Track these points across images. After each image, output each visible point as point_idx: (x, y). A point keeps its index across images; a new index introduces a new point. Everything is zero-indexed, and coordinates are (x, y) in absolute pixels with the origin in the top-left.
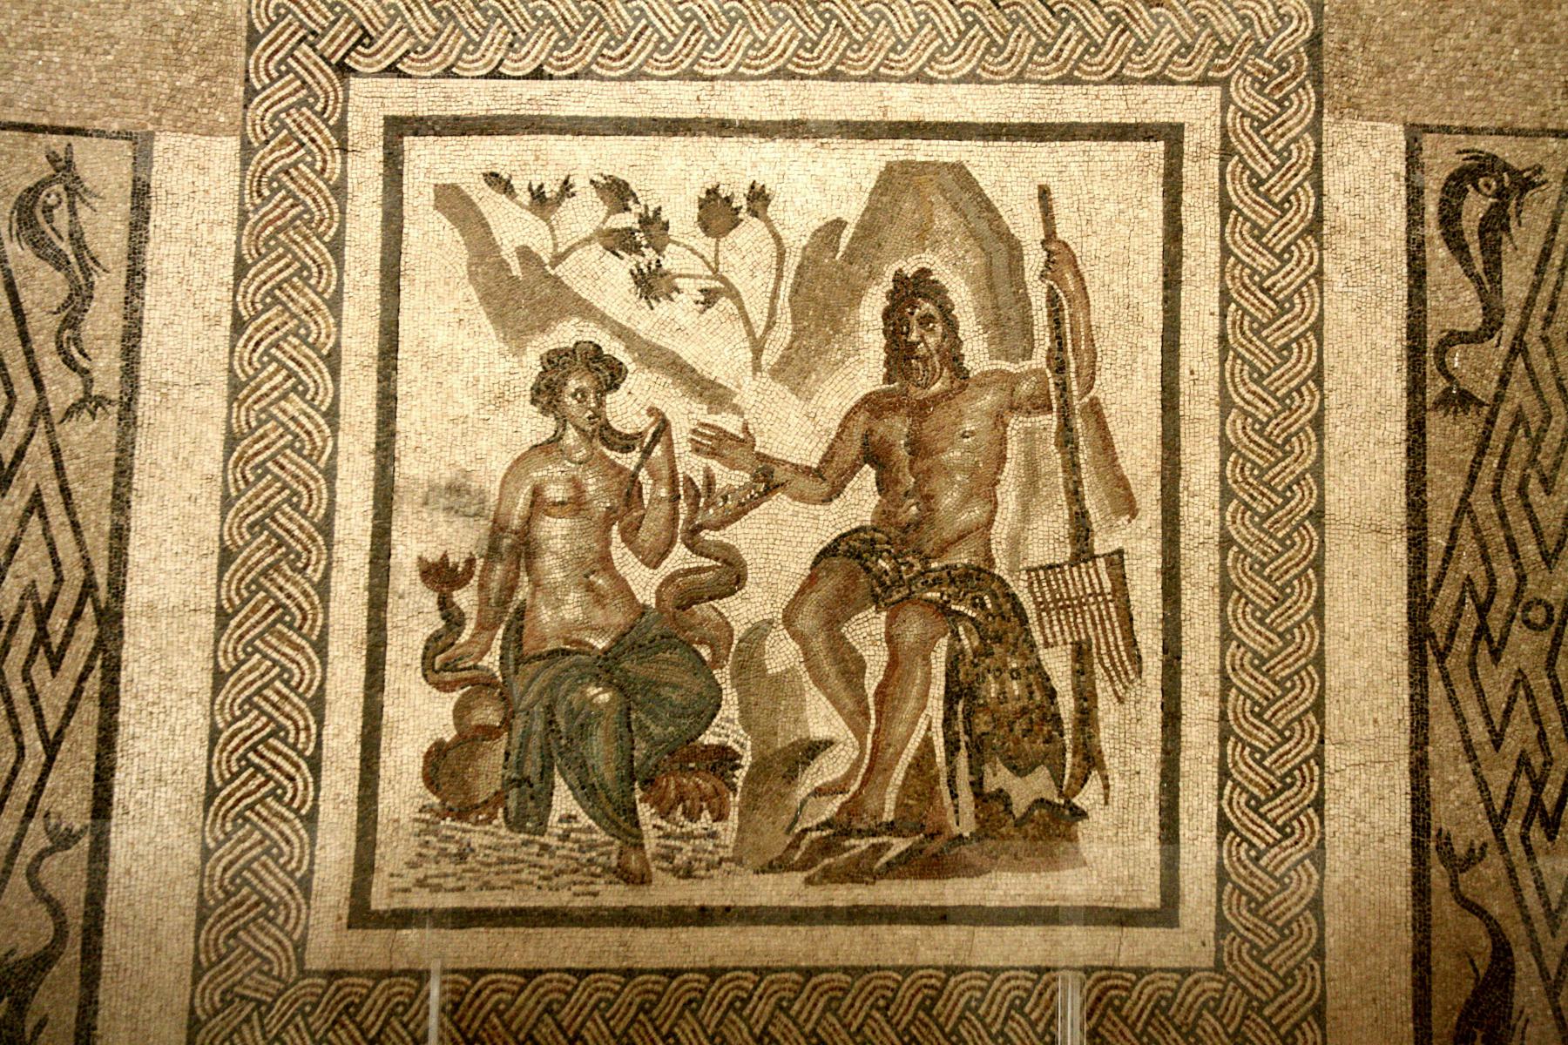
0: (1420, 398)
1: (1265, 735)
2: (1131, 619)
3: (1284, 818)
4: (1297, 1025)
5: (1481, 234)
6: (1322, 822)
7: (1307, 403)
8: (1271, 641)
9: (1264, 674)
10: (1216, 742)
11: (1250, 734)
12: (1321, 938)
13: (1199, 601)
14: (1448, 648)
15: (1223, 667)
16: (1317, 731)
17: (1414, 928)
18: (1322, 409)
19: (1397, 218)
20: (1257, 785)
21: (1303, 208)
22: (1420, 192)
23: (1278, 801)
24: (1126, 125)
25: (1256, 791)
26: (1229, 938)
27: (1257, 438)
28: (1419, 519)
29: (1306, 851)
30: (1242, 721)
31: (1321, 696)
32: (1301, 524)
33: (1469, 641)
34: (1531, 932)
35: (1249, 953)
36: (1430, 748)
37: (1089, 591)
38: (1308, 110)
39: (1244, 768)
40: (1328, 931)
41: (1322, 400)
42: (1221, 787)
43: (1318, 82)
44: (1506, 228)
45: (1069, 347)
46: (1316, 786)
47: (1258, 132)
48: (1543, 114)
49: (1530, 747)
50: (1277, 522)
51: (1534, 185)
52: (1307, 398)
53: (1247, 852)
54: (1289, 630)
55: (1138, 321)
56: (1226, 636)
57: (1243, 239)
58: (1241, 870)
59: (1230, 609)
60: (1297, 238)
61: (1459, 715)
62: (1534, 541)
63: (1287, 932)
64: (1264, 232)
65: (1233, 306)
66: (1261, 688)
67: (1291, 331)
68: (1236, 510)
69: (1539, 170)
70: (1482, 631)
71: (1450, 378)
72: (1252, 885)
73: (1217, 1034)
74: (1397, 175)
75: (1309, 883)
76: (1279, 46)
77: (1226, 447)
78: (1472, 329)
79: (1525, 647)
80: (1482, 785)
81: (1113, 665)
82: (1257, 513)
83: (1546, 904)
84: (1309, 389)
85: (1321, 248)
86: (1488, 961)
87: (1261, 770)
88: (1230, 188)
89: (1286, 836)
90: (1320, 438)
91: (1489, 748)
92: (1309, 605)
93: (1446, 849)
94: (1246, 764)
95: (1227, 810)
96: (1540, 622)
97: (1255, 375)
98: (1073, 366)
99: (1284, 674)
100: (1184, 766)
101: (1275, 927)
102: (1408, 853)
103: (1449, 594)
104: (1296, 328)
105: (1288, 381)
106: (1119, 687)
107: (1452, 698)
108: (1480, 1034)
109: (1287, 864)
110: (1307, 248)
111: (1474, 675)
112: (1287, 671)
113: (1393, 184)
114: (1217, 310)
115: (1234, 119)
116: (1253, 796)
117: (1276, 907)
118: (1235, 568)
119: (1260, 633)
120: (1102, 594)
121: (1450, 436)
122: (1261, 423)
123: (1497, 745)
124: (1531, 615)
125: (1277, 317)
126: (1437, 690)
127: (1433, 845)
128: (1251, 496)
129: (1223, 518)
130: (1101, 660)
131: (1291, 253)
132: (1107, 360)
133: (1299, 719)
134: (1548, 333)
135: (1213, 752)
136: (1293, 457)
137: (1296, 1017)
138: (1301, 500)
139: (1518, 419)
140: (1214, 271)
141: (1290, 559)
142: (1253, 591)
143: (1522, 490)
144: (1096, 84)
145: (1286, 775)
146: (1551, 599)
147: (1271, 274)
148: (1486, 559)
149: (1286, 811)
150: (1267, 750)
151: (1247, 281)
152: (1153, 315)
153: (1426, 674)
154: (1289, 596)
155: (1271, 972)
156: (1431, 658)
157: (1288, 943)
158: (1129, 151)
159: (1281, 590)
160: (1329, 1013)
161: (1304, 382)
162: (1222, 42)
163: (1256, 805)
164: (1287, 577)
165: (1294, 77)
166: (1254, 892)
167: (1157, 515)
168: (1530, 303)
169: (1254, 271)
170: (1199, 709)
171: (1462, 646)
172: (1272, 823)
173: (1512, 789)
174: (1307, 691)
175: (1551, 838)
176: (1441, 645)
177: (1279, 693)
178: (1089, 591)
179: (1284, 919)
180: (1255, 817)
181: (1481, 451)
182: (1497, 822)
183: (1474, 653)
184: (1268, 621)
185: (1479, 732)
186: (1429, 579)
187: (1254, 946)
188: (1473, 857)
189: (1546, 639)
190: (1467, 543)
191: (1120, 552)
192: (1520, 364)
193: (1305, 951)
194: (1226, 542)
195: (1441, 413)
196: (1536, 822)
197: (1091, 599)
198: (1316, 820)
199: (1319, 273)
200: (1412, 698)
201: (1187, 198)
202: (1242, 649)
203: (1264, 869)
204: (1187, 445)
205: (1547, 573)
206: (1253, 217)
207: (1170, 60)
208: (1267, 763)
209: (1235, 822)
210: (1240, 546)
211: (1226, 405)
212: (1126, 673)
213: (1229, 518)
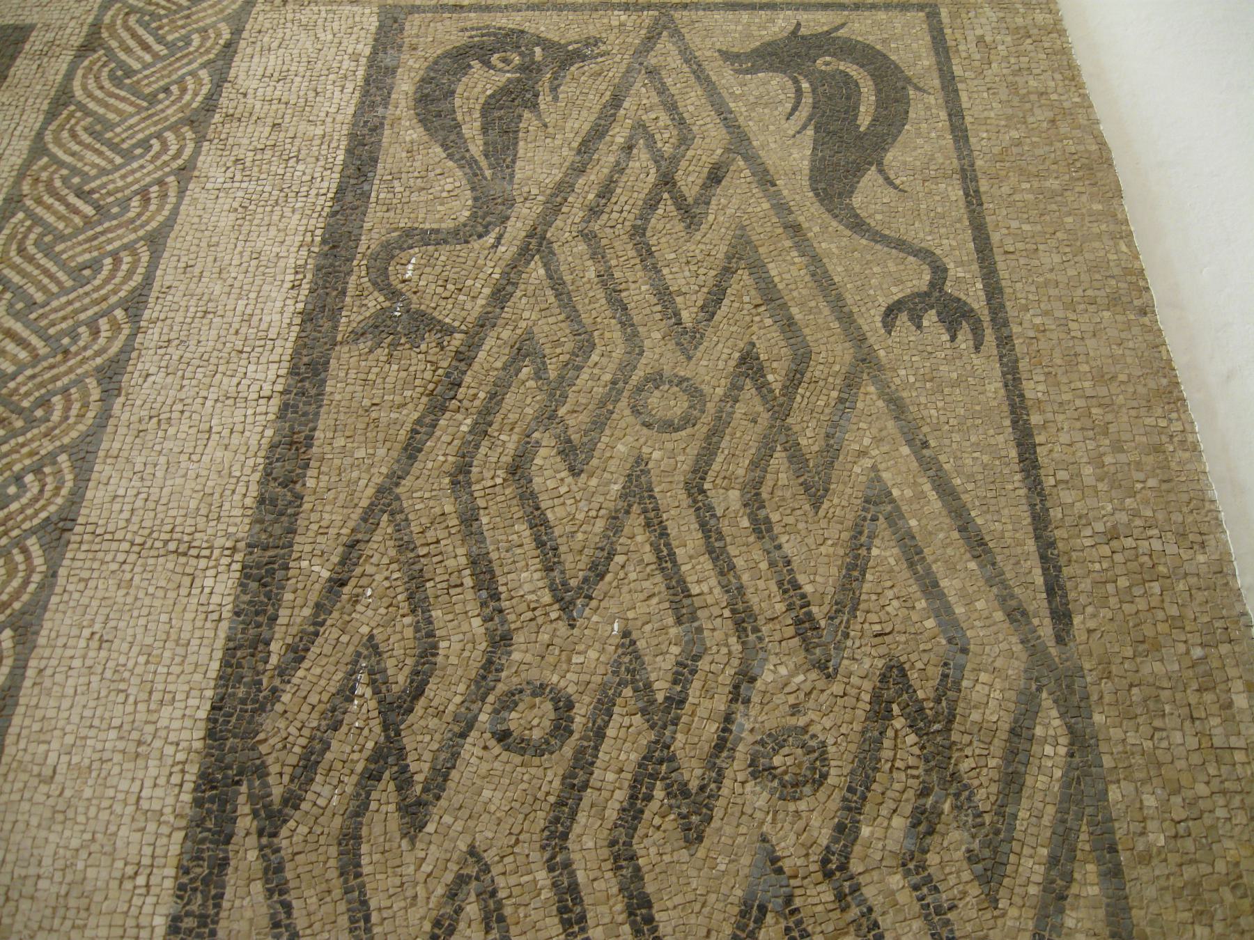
14: (292, 801)
18: (128, 348)
21: (187, 97)
28: (277, 530)
41: (132, 336)
51: (584, 58)
62: (535, 564)
67: (110, 241)
70: (388, 757)
71: (394, 294)
78: (448, 224)
96: (536, 734)
103: (318, 676)
105: (77, 312)
111: (350, 866)
124: (514, 720)
134: (596, 226)
138: (35, 500)
139: (523, 350)
143: (518, 469)
146: (569, 684)
147: (103, 172)
148: (418, 602)
153: (224, 864)
156: (245, 822)
168: (563, 189)
176: (277, 792)
181: (438, 406)
183: (360, 809)
186: (275, 647)
189: (550, 775)
190: (380, 567)
195: (364, 346)
205: (562, 628)
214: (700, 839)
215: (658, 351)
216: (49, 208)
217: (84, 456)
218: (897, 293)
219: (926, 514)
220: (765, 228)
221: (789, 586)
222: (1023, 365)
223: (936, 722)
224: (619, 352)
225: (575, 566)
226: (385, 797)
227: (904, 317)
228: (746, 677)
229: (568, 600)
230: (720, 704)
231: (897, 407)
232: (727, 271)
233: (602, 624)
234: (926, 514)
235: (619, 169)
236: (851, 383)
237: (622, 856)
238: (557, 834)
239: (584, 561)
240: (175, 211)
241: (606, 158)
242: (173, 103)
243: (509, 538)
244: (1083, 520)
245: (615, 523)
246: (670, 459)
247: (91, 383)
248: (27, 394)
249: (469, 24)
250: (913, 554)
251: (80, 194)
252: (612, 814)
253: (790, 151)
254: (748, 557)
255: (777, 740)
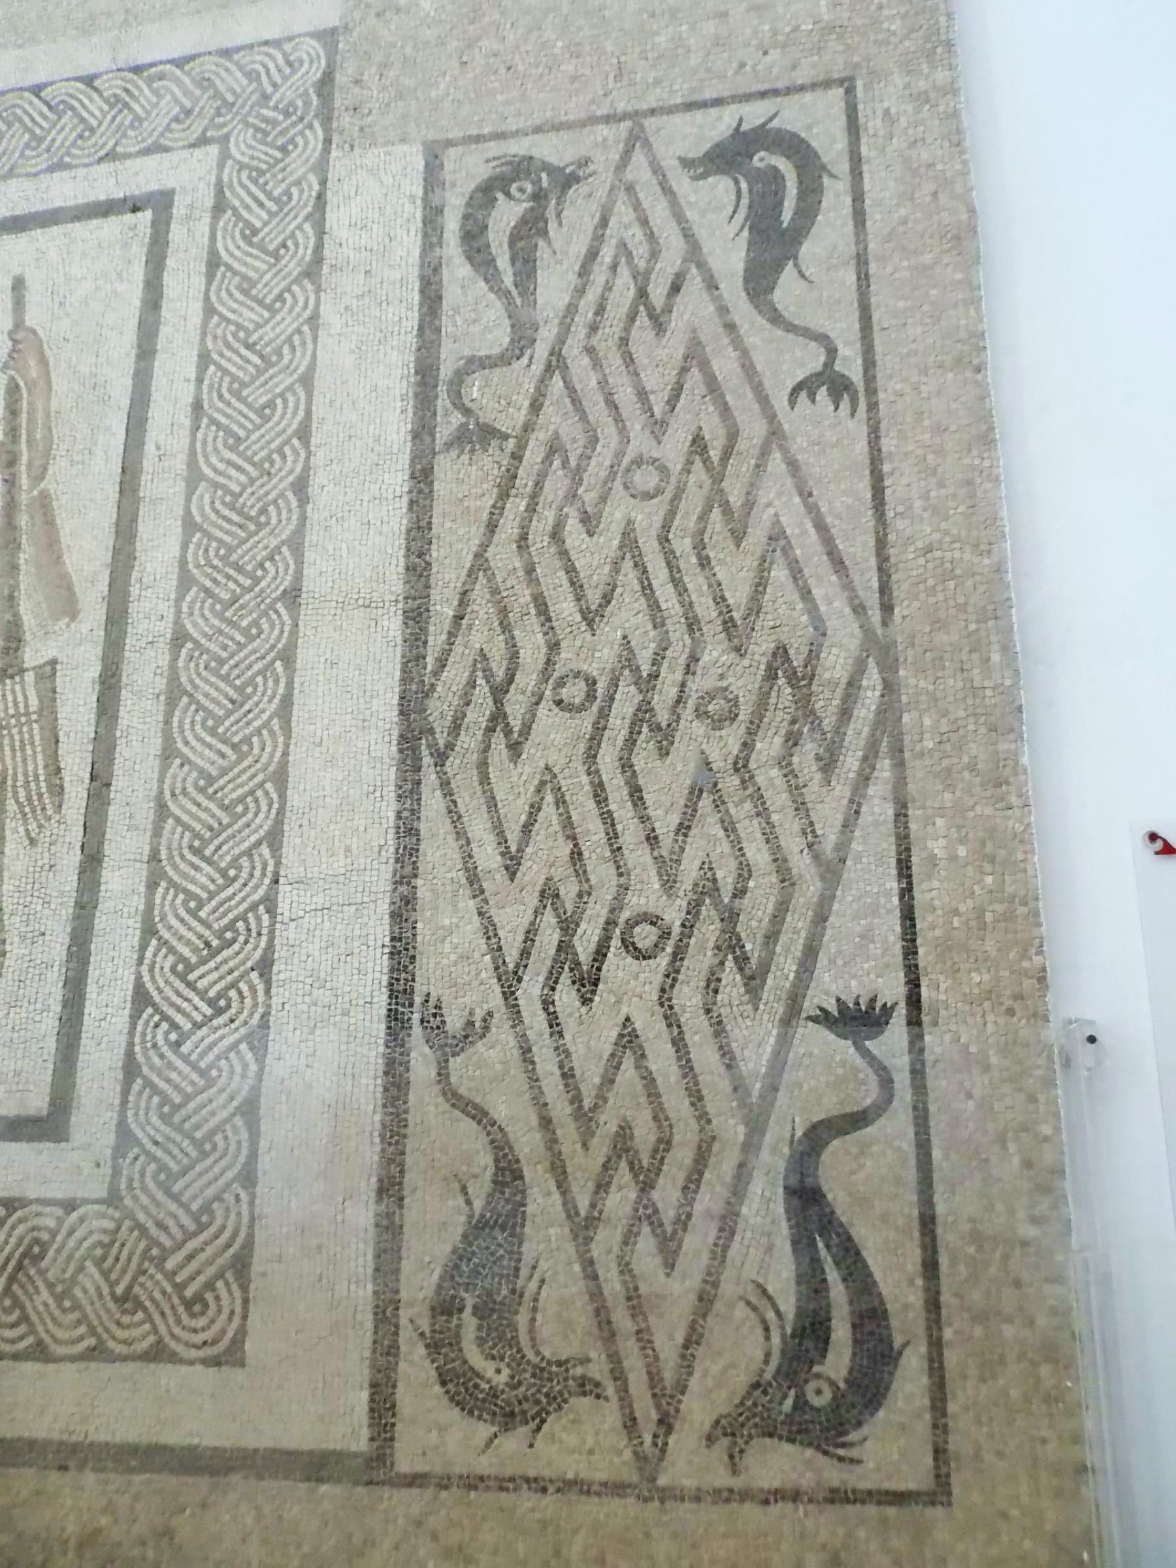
0: (428, 440)
1: (204, 877)
2: (57, 741)
3: (217, 987)
4: (210, 1285)
5: (512, 244)
6: (268, 991)
7: (289, 463)
8: (223, 756)
9: (210, 798)
10: (142, 889)
11: (185, 876)
12: (253, 1156)
13: (139, 716)
14: (450, 746)
15: (161, 792)
16: (270, 868)
17: (382, 1138)
18: (307, 468)
19: (409, 245)
20: (188, 943)
21: (301, 251)
22: (440, 211)
23: (212, 964)
24: (113, 200)
25: (186, 952)
26: (131, 1155)
27: (226, 512)
28: (420, 586)
29: (243, 1031)
30: (177, 859)
31: (279, 821)
32: (272, 606)
33: (479, 734)
34: (552, 1142)
35: (155, 1177)
36: (419, 882)
37: (11, 711)
38: (314, 150)
39: (174, 922)
40: (263, 1144)
41: (308, 459)
42: (143, 948)
43: (327, 120)
44: (544, 233)
45: (24, 438)
46: (263, 944)
47: (256, 182)
48: (592, 102)
49: (558, 873)
50: (242, 607)
52: (290, 459)
53: (167, 1033)
54: (247, 740)
55: (104, 400)
56: (168, 753)
57: (231, 295)
58: (157, 1061)
59: (176, 720)
60: (293, 282)
61: (461, 834)
62: (571, 597)
63: (208, 1147)
64: (253, 284)
65: (212, 368)
66: (204, 816)
67: (277, 385)
68: (194, 601)
69: (587, 161)
70: (498, 718)
71: (467, 412)
72: (168, 1081)
73: (101, 1296)
74: (412, 198)
75: (244, 1076)
76: (286, 93)
77: (190, 525)
78: (496, 351)
79: (556, 736)
80: (490, 930)
81: (29, 799)
82: (220, 601)
83: (577, 1099)
84: (293, 448)
85: (318, 290)
86: (488, 1186)
87: (195, 924)
88: (220, 245)
89: (220, 1012)
90: (303, 501)
91: (501, 876)
92: (274, 706)
93: (435, 1022)
94: (177, 916)
95: (146, 978)
96: (577, 701)
97: (231, 441)
98: (24, 459)
99: (234, 796)
100: (100, 922)
101: (192, 1139)
102: (380, 1029)
103: (455, 675)
104: (282, 382)
105: (269, 443)
106: (33, 826)
107: (453, 812)
108: (470, 1301)
109: (216, 1050)
110: (303, 293)
111: (485, 779)
112: (240, 791)
113: (408, 207)
114: (193, 376)
115: (230, 174)
116: (182, 959)
117: (196, 1111)
118: (187, 668)
119: (210, 746)
120: (27, 714)
121: (463, 481)
122: (232, 494)
123: (512, 869)
124: (565, 693)
125: (260, 372)
126: (433, 802)
127: (416, 1017)
128: (215, 581)
129: (179, 611)
130: (15, 793)
131: (284, 302)
132: (63, 447)
133: (249, 853)
134: (595, 341)
135: (138, 902)
136: (268, 529)
137: (210, 1271)
138: (275, 578)
139: (554, 448)
140: (194, 334)
141: (255, 651)
142: (207, 695)
143: (556, 535)
144: (86, 165)
145: (227, 928)
146: (593, 670)
147: (258, 326)
148: (506, 627)
149: (221, 978)
150: (205, 895)
151: (230, 338)
152: (121, 392)
153: (419, 783)
154: (249, 697)
155: (181, 1205)
156: (427, 760)
157: (208, 1162)
158: (112, 226)
159: (240, 690)
160: (256, 1267)
161: (287, 442)
162: (224, 100)
163: (184, 971)
164: (250, 673)
165: (301, 119)
166: (168, 1089)
167: (101, 614)
168: (571, 309)
169: (239, 326)
170: (125, 846)
171: (469, 741)
172: (202, 994)
173: (530, 935)
174: (262, 816)
175: (586, 1001)
176: (441, 743)
177: (226, 821)
178: (11, 711)
179: (206, 1128)
180: (181, 987)
181: (504, 495)
182: (509, 981)
183: (487, 749)
184: (221, 730)
185: (488, 857)
186: (429, 660)
187: (164, 1168)
188: (475, 1030)
189: (585, 723)
190: (482, 607)
191: (54, 662)
192: (557, 383)
193: (229, 1175)
194: (179, 638)
195: (454, 453)
196: (566, 978)
197: (13, 721)
198: (260, 988)
199: (314, 320)
200: (399, 816)
201: (170, 263)
202: (186, 768)
203: (185, 1059)
204: (145, 530)
205: (588, 635)
206: (243, 269)
207: (168, 128)
208: (202, 914)
209: (155, 994)
210: (196, 642)
211: (194, 477)
212: (43, 809)
213: (185, 609)
214: (668, 754)
215: (640, 441)
216: (229, 360)
217: (296, 544)
218: (800, 375)
219: (807, 546)
220: (711, 331)
221: (720, 600)
222: (883, 426)
223: (803, 681)
224: (614, 442)
225: (593, 597)
226: (499, 742)
227: (803, 395)
228: (694, 659)
229: (590, 618)
230: (678, 676)
231: (793, 466)
232: (684, 370)
233: (610, 631)
234: (807, 546)
235: (608, 287)
236: (764, 452)
237: (626, 766)
238: (591, 756)
239: (599, 593)
240: (314, 356)
241: (599, 277)
242: (292, 257)
243: (554, 582)
244: (910, 540)
245: (616, 567)
246: (647, 518)
247: (290, 495)
248: (252, 507)
249: (491, 155)
250: (796, 572)
251: (249, 347)
252: (620, 742)
253: (729, 255)
254: (695, 582)
255: (711, 696)
